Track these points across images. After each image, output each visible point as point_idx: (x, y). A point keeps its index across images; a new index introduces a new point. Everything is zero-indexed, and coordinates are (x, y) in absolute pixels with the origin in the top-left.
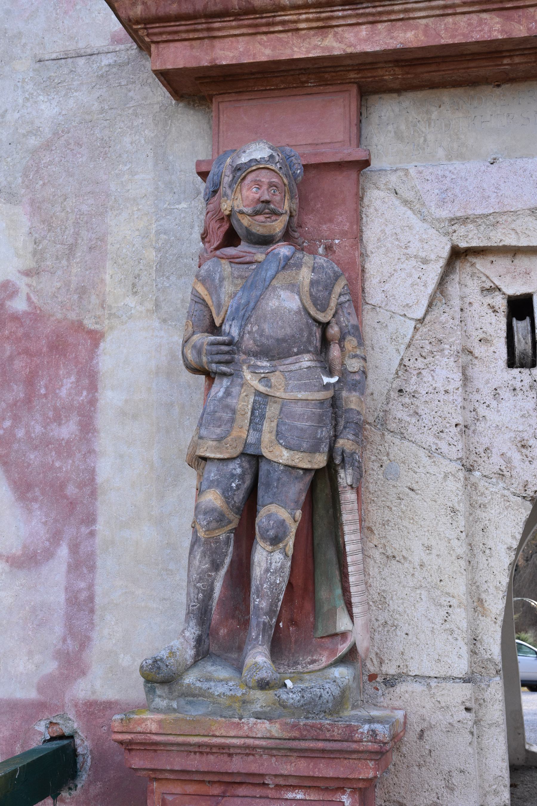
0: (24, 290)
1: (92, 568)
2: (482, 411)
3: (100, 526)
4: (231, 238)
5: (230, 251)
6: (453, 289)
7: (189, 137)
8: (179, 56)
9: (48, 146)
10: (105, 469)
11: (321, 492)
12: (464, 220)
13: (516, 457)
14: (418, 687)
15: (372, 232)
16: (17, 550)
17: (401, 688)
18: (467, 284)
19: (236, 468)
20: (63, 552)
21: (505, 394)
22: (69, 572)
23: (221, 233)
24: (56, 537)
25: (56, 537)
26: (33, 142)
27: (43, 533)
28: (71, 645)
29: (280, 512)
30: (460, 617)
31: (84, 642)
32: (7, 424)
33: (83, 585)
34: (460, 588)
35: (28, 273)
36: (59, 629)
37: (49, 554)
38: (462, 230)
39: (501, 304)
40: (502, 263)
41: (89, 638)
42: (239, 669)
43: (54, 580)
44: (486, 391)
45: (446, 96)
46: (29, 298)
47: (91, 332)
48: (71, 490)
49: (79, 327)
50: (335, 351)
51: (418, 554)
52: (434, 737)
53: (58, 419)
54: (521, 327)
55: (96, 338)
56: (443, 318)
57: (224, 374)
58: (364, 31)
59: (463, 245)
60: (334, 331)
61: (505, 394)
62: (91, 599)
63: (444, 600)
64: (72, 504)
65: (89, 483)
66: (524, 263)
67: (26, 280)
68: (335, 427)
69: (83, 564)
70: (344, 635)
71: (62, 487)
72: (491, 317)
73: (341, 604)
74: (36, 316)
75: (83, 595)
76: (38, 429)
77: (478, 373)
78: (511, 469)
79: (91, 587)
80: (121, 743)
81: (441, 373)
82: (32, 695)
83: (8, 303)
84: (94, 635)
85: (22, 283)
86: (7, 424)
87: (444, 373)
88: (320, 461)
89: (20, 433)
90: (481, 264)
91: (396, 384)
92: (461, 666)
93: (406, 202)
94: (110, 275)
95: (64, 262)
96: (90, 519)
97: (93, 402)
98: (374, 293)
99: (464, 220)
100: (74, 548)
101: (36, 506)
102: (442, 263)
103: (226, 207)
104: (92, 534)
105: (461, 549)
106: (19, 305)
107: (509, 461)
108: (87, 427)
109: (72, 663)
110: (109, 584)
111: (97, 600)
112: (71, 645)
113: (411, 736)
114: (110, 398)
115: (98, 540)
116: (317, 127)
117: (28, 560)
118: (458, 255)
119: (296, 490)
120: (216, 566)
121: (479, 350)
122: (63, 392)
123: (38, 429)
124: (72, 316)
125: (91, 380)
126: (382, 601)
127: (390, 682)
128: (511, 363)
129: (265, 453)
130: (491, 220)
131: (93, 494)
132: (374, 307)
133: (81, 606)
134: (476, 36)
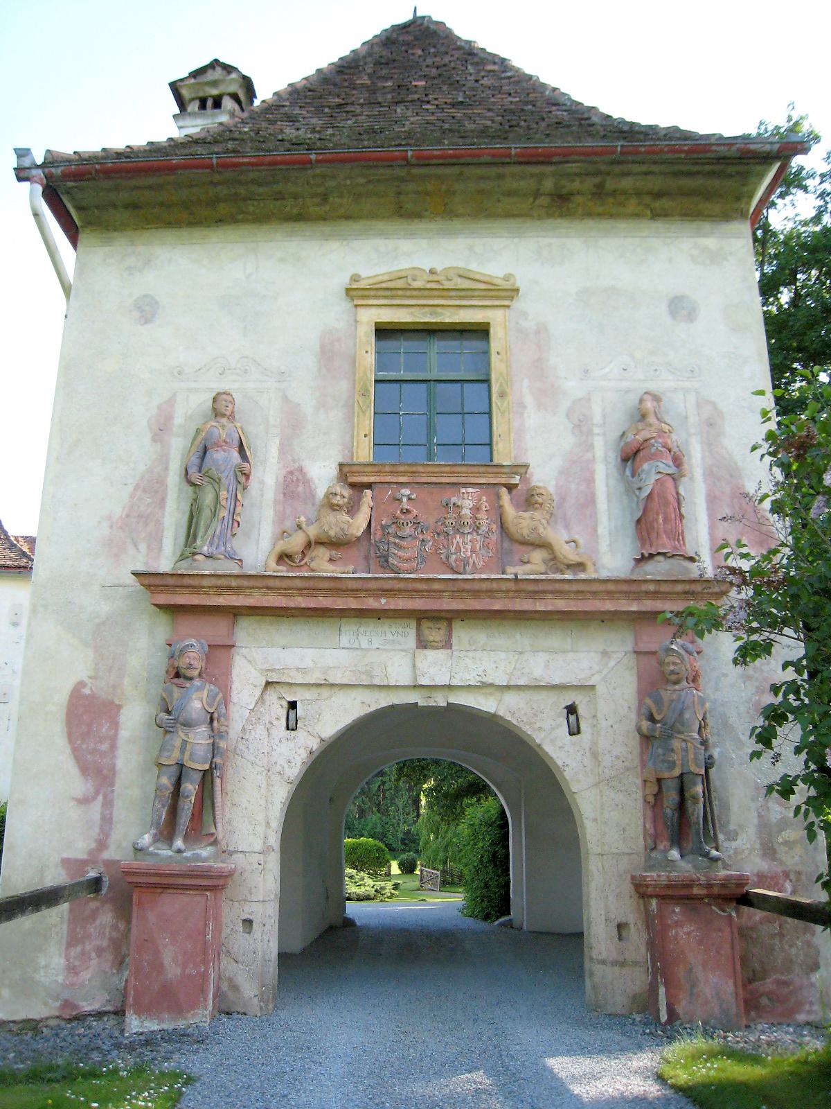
0: (89, 685)
1: (112, 806)
2: (274, 747)
3: (116, 788)
4: (178, 675)
5: (176, 681)
6: (267, 697)
7: (162, 628)
8: (163, 599)
9: (103, 623)
10: (120, 763)
11: (207, 778)
12: (272, 670)
13: (286, 766)
14: (241, 855)
15: (236, 672)
16: (80, 796)
17: (235, 856)
18: (272, 696)
19: (174, 769)
20: (100, 798)
21: (284, 740)
22: (103, 806)
23: (173, 673)
24: (97, 793)
25: (97, 793)
26: (97, 621)
27: (92, 790)
28: (101, 837)
29: (190, 788)
30: (260, 829)
31: (107, 835)
32: (79, 742)
33: (108, 812)
34: (260, 817)
35: (90, 677)
36: (97, 830)
37: (94, 799)
38: (270, 674)
39: (286, 705)
40: (286, 688)
41: (110, 835)
42: (171, 846)
43: (96, 808)
44: (276, 740)
45: (268, 619)
46: (91, 688)
47: (116, 705)
48: (105, 772)
49: (112, 703)
50: (215, 724)
51: (245, 804)
52: (246, 875)
53: (101, 742)
54: (292, 713)
55: (119, 707)
56: (261, 709)
57: (171, 732)
58: (234, 597)
59: (270, 680)
60: (216, 715)
61: (284, 740)
62: (111, 818)
63: (253, 823)
64: (105, 778)
65: (113, 770)
66: (294, 688)
67: (91, 680)
68: (213, 754)
69: (108, 803)
70: (212, 834)
71: (101, 771)
72: (281, 709)
73: (212, 823)
74: (93, 696)
75: (109, 816)
76: (92, 745)
77: (274, 732)
78: (283, 771)
79: (111, 813)
80: (123, 872)
81: (259, 732)
82: (84, 856)
83: (83, 690)
84: (112, 833)
85: (89, 682)
86: (79, 742)
87: (260, 731)
88: (207, 767)
89: (84, 746)
90: (278, 687)
91: (241, 735)
92: (258, 846)
93: (249, 661)
94: (126, 681)
95: (107, 674)
96: (112, 784)
97: (116, 735)
98: (235, 697)
99: (272, 670)
100: (105, 797)
101: (89, 778)
102: (262, 687)
103: (176, 664)
104: (113, 791)
105: (263, 802)
106: (87, 691)
107: (283, 768)
108: (113, 747)
109: (102, 844)
110: (120, 811)
111: (114, 819)
112: (101, 837)
113: (237, 874)
114: (124, 734)
115: (115, 794)
116: (216, 629)
117: (84, 801)
118: (268, 684)
119: (197, 777)
120: (163, 806)
121: (275, 722)
122: (104, 730)
123: (92, 745)
124: (109, 697)
125: (115, 725)
126: (230, 822)
127: (231, 853)
128: (288, 729)
129: (185, 763)
130: (281, 671)
131: (114, 774)
132: (234, 703)
133: (107, 820)
134: (277, 605)
